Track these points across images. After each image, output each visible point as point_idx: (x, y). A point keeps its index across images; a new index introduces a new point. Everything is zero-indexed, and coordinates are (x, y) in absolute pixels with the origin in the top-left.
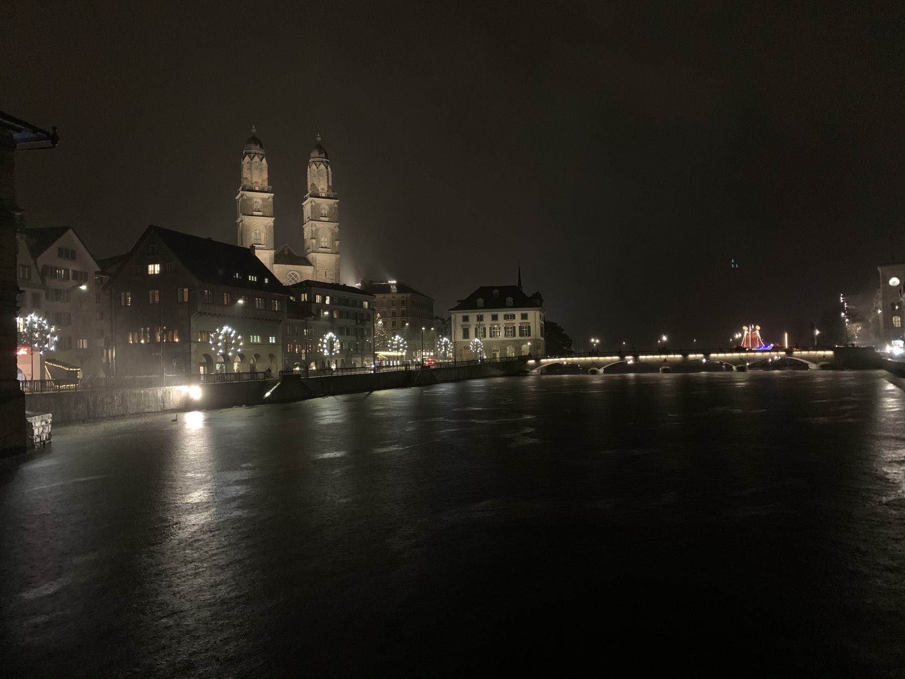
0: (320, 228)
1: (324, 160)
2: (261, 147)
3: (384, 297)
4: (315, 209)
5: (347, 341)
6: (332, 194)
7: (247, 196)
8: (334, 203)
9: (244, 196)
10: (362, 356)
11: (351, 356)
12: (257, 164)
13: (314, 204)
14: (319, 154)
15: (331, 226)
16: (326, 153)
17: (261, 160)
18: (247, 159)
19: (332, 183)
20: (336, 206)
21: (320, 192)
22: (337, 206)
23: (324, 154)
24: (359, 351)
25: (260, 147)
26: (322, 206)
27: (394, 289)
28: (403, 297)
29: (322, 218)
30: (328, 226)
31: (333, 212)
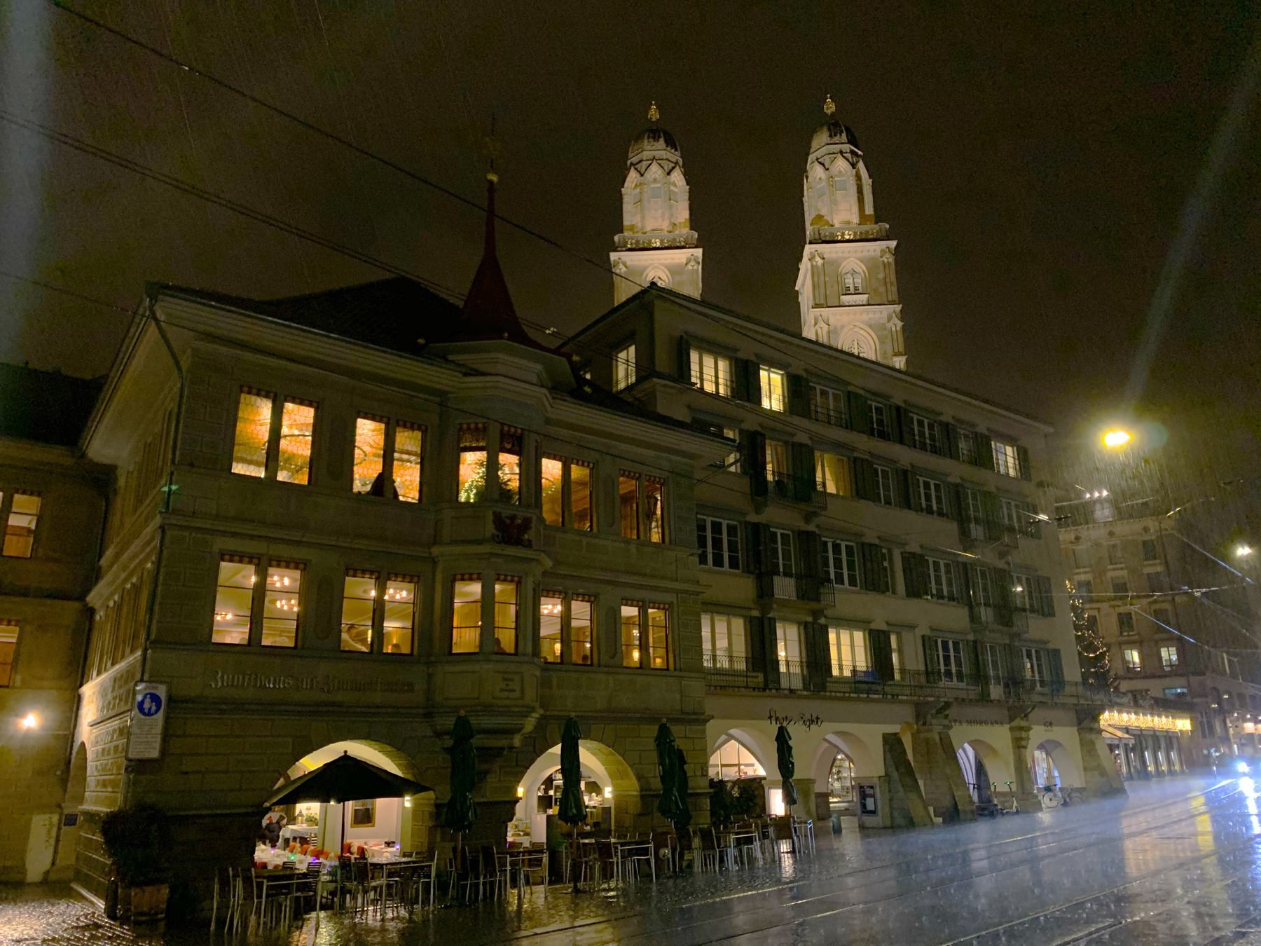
0: (843, 327)
1: (847, 147)
2: (671, 143)
3: (1077, 538)
4: (821, 274)
5: (912, 627)
6: (873, 228)
7: (629, 263)
8: (882, 251)
9: (621, 266)
10: (1011, 719)
11: (943, 709)
12: (659, 185)
13: (820, 262)
14: (830, 136)
15: (871, 316)
16: (848, 131)
17: (669, 174)
18: (633, 176)
19: (875, 207)
20: (889, 258)
21: (838, 229)
22: (891, 260)
23: (844, 135)
24: (996, 691)
25: (666, 141)
26: (847, 266)
27: (1104, 514)
28: (1146, 529)
29: (846, 299)
30: (865, 317)
31: (881, 276)
